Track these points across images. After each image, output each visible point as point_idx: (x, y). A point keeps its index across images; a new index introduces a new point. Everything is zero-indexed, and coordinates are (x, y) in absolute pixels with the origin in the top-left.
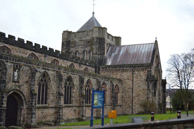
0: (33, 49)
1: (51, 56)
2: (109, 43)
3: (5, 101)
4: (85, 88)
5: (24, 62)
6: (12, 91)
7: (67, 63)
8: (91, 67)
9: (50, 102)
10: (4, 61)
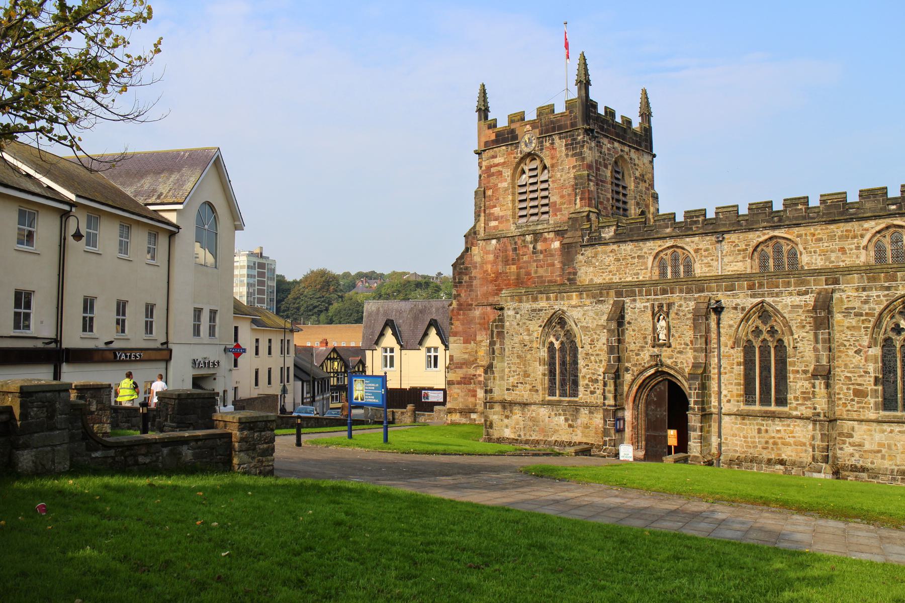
0: (889, 210)
3: (609, 392)
5: (681, 291)
6: (651, 367)
10: (627, 300)
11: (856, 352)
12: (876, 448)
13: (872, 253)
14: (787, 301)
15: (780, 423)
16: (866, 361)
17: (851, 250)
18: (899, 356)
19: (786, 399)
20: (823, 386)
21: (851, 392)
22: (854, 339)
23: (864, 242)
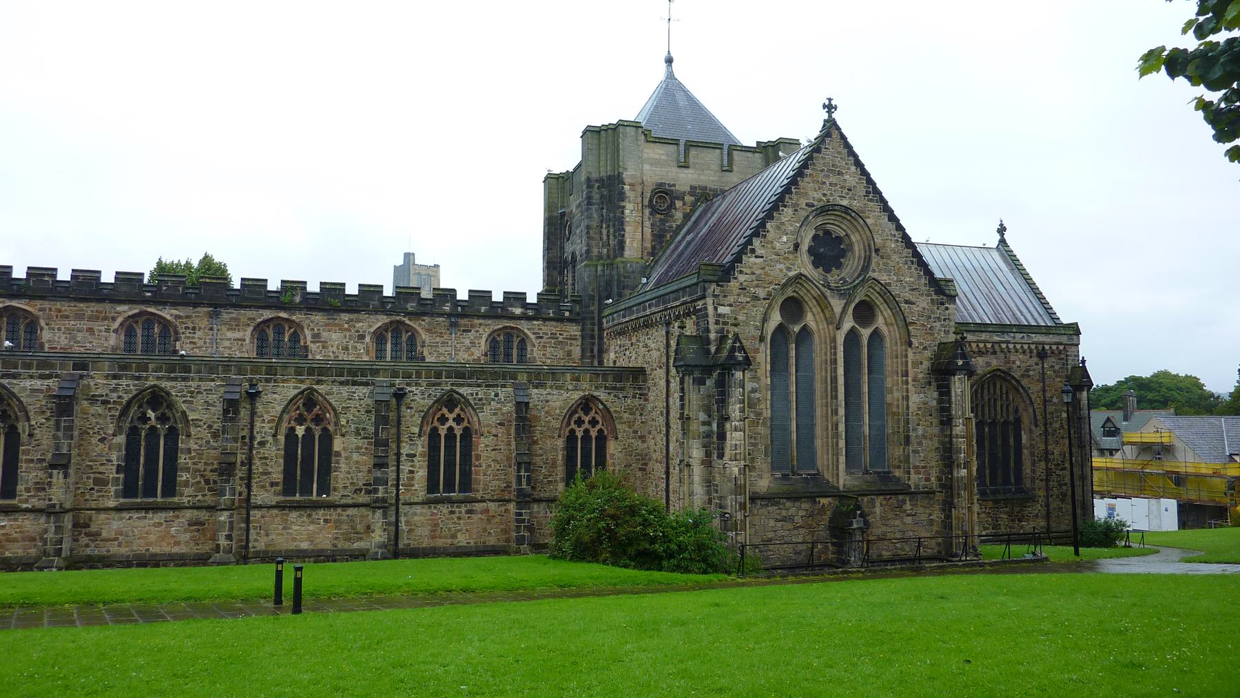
0: (144, 297)
1: (250, 307)
2: (691, 187)
4: (292, 429)
7: (359, 325)
8: (545, 320)
9: (28, 490)
11: (99, 440)
12: (113, 535)
13: (123, 338)
14: (28, 383)
15: (6, 518)
16: (109, 449)
17: (101, 331)
18: (143, 443)
19: (15, 490)
20: (61, 476)
21: (92, 481)
22: (98, 426)
23: (116, 325)
